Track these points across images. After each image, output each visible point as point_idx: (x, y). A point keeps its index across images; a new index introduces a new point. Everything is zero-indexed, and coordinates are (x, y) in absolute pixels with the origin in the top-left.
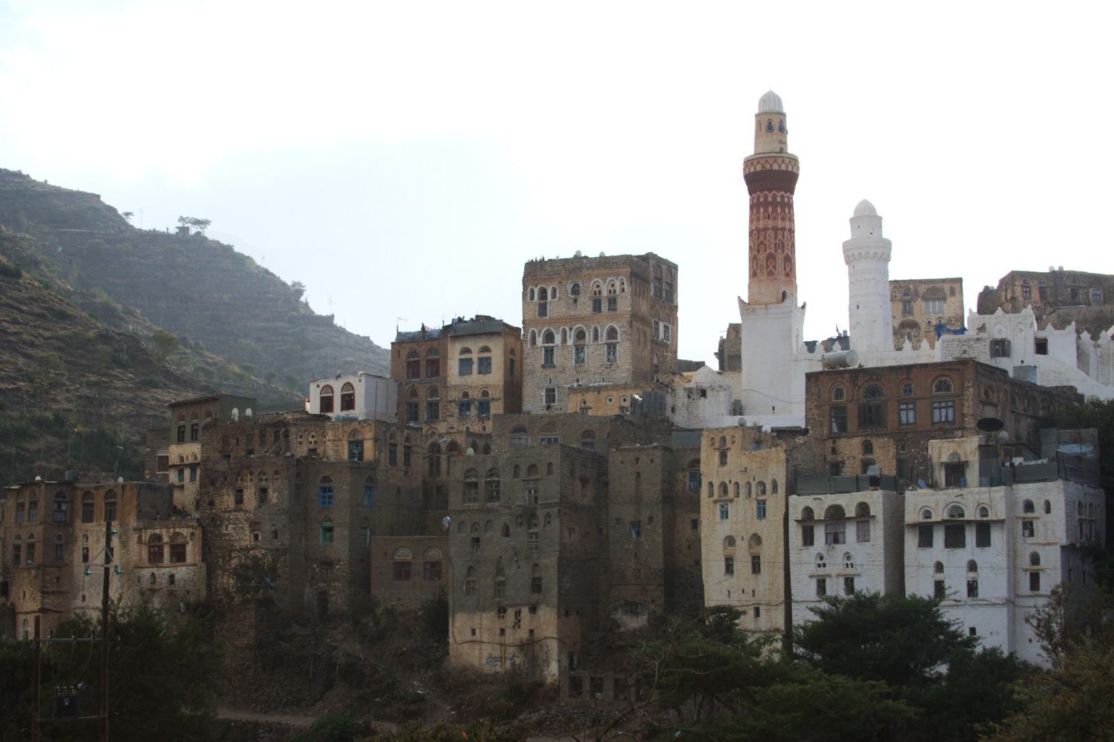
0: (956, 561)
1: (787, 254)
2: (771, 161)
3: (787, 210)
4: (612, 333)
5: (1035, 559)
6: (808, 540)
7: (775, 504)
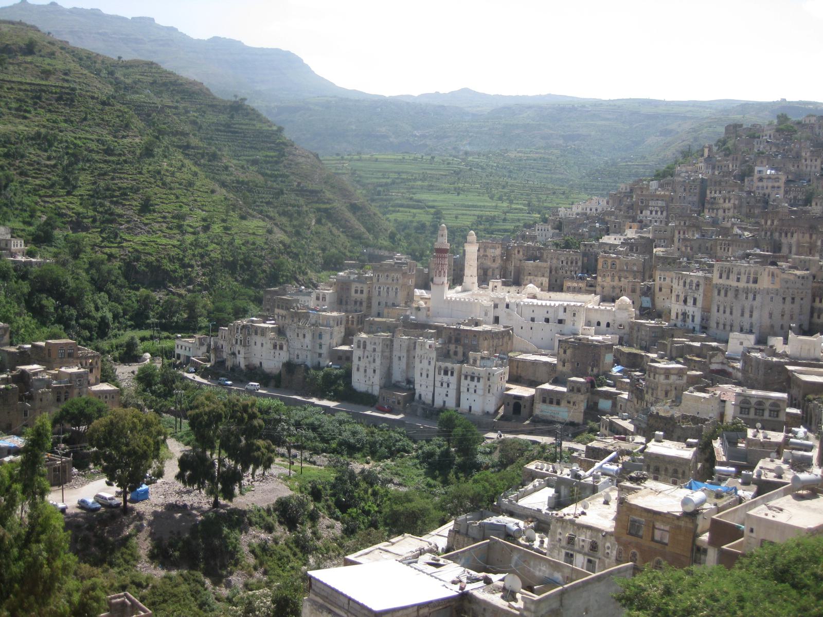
0: (473, 384)
4: (397, 289)
5: (490, 386)
6: (439, 374)
7: (433, 363)
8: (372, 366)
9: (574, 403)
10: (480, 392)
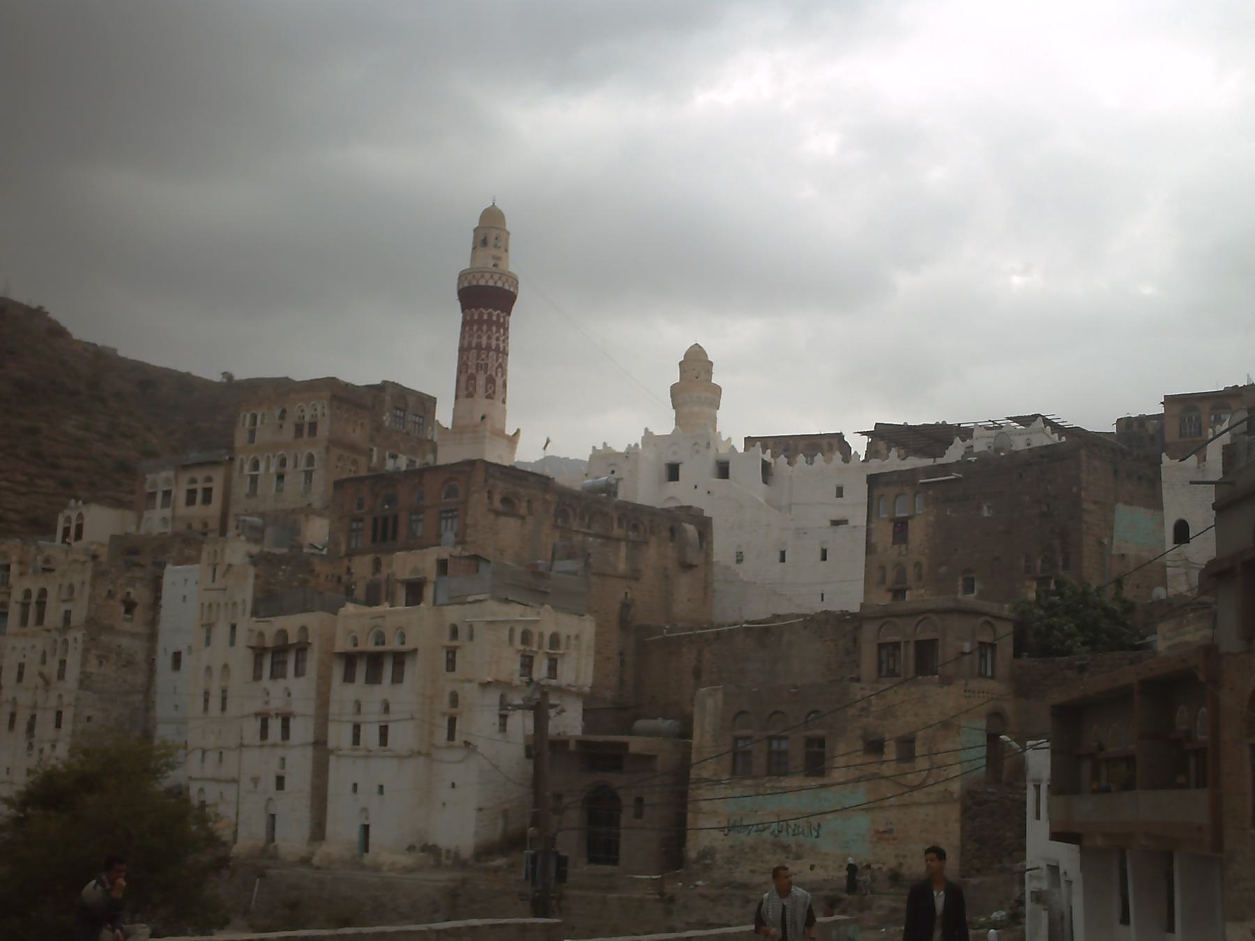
0: (373, 696)
1: (491, 375)
2: (478, 276)
3: (502, 331)
4: (310, 460)
5: (454, 700)
8: (53, 702)
9: (907, 746)
10: (402, 737)
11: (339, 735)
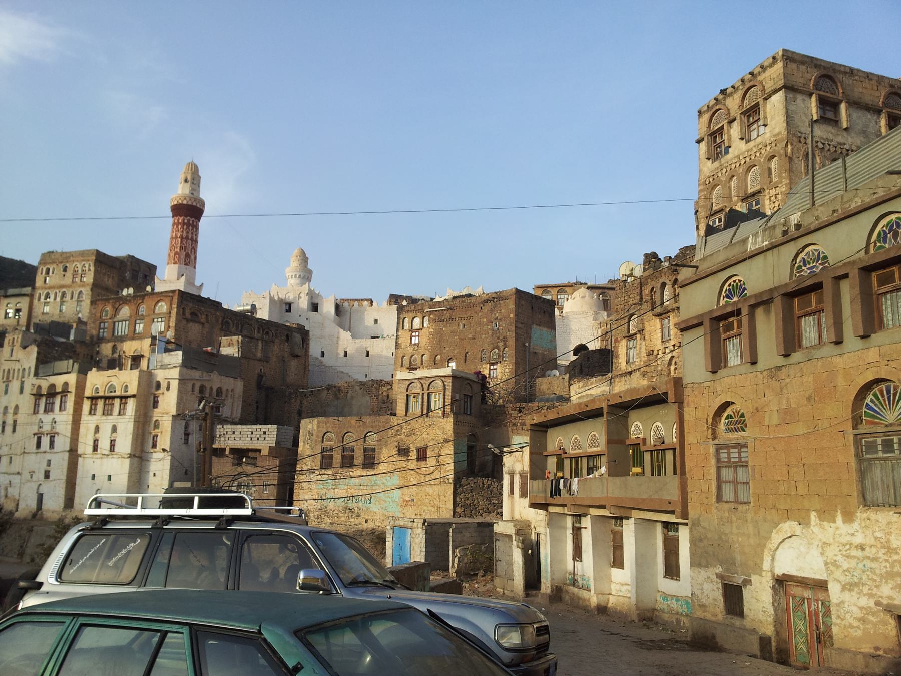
1: (188, 253)
11: (85, 446)
